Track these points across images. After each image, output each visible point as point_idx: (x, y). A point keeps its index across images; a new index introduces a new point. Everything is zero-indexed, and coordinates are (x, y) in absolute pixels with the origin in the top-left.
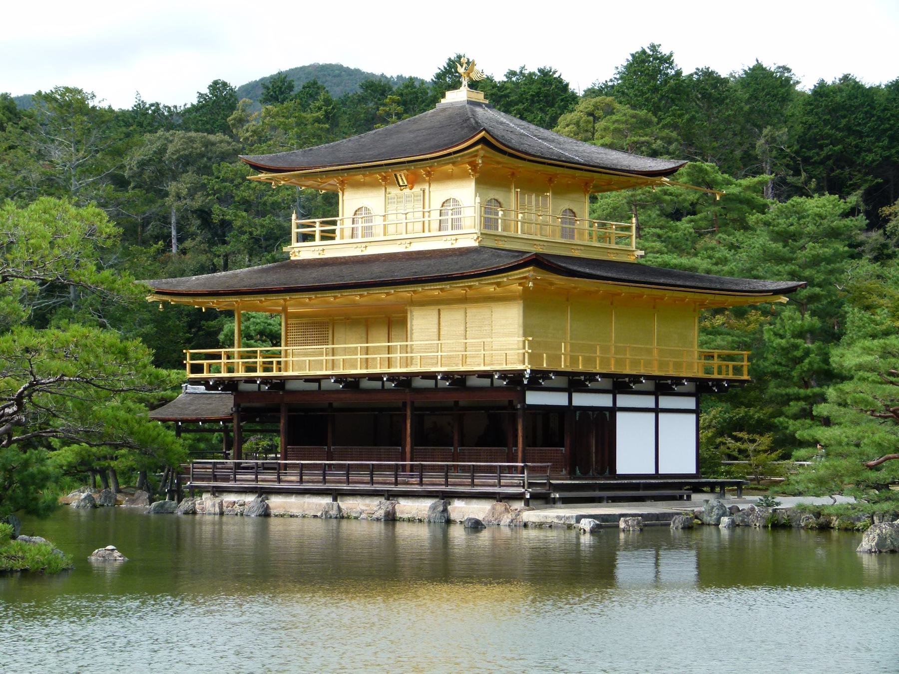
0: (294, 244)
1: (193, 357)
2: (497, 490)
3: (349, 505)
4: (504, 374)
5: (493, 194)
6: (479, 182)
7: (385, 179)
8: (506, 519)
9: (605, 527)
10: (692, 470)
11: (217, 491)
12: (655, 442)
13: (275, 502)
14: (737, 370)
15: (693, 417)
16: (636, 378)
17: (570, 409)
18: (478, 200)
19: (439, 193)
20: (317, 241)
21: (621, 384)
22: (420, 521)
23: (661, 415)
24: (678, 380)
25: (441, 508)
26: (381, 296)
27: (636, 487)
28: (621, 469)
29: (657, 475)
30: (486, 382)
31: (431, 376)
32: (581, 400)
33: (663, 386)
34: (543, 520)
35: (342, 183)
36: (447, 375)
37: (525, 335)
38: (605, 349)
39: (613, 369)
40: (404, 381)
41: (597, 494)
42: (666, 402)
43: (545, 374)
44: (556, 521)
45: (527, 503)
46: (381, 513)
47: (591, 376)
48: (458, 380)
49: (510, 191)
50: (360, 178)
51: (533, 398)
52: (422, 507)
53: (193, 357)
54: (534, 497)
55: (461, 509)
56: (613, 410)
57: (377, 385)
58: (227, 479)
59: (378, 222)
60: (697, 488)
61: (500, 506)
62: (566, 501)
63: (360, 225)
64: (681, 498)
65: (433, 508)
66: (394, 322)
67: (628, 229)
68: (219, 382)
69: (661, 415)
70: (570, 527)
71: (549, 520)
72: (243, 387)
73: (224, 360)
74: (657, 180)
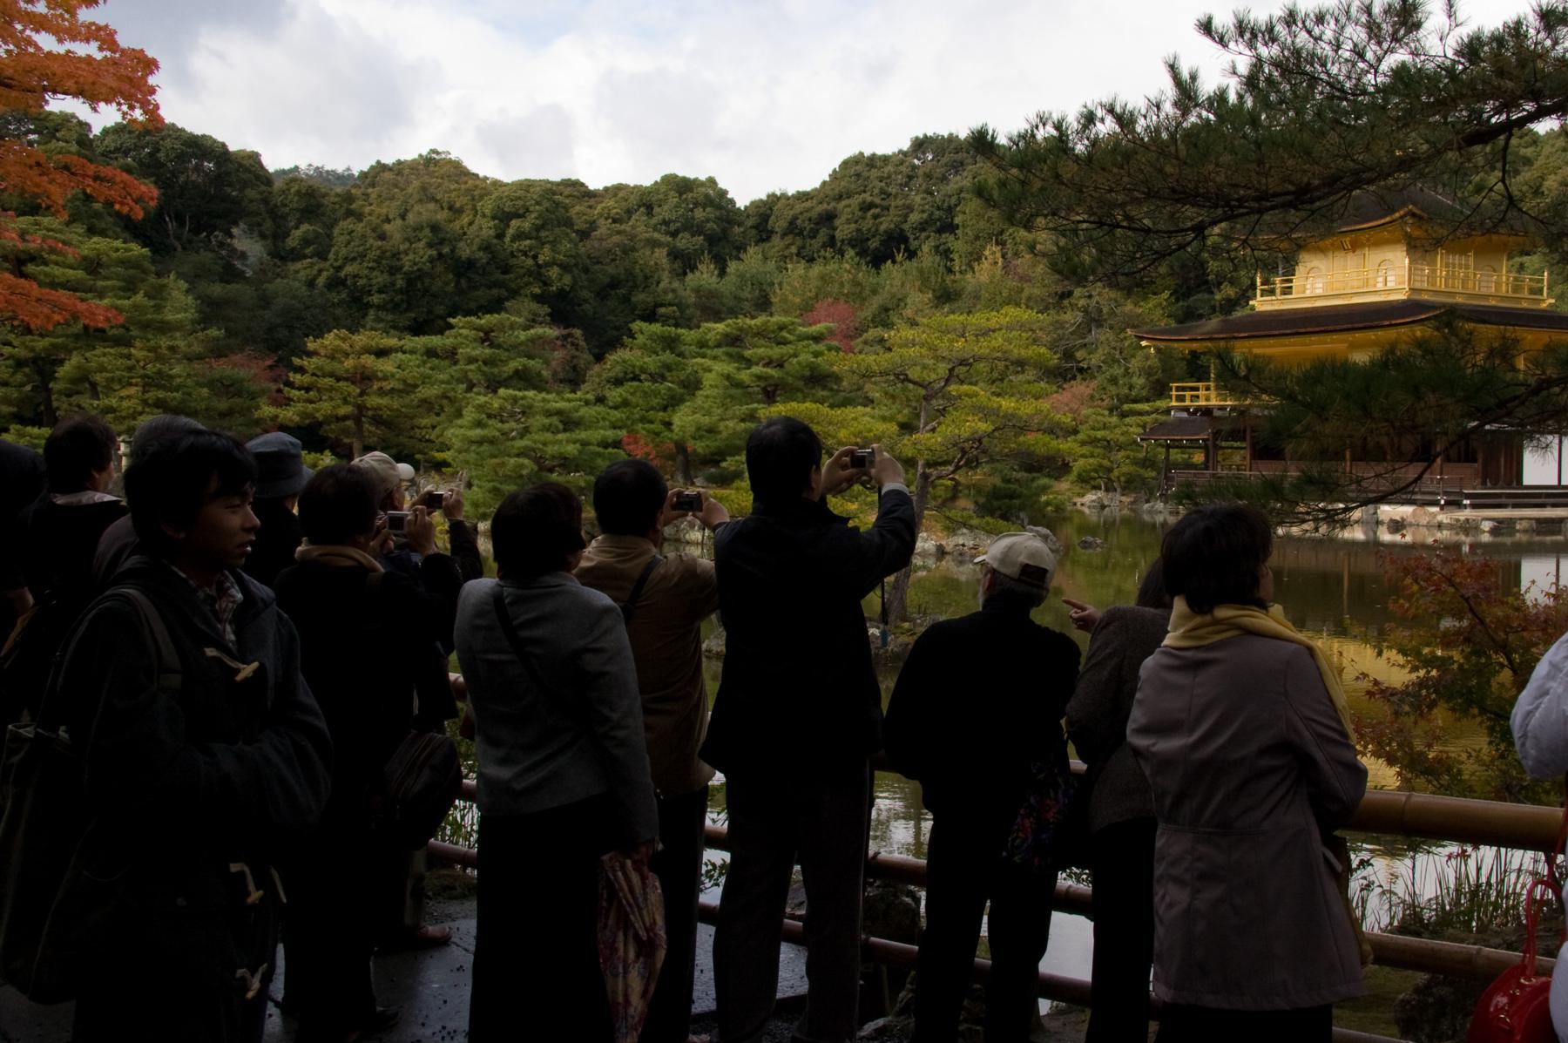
1: (1178, 389)
8: (1424, 521)
9: (1501, 527)
19: (1374, 257)
28: (1527, 481)
29: (1560, 486)
41: (1503, 501)
45: (1442, 508)
53: (1178, 389)
54: (1448, 503)
55: (1388, 511)
61: (1420, 510)
62: (1474, 506)
68: (1198, 409)
72: (1217, 413)
73: (1201, 393)
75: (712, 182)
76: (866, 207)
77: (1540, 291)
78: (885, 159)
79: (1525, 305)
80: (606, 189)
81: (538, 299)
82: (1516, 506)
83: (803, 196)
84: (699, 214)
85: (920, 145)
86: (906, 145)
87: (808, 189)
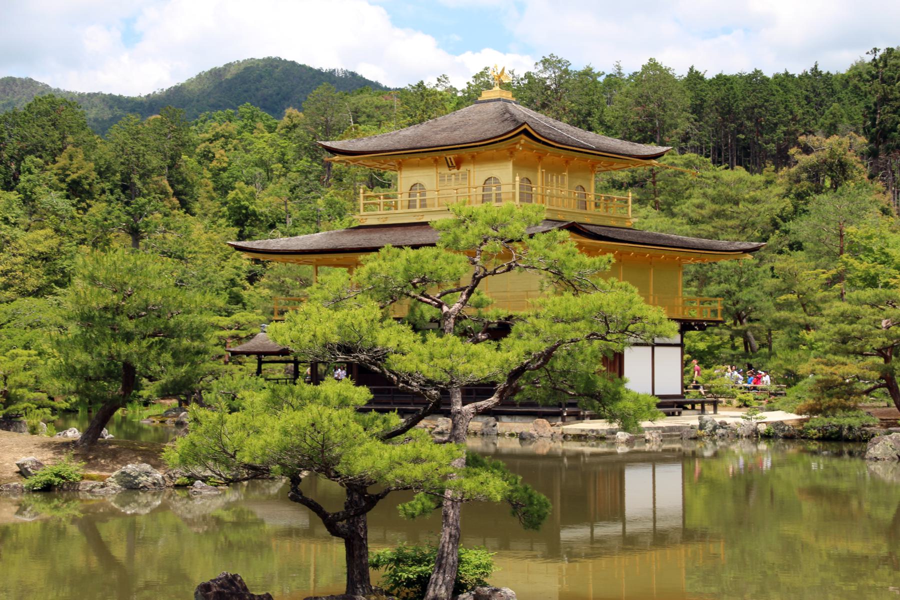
0: (362, 213)
5: (526, 174)
6: (514, 165)
7: (436, 161)
10: (679, 393)
12: (654, 371)
14: (714, 311)
15: (679, 349)
18: (517, 179)
22: (475, 434)
23: (656, 349)
25: (492, 424)
34: (579, 432)
35: (400, 166)
44: (590, 434)
45: (563, 420)
49: (537, 171)
50: (416, 159)
54: (569, 415)
59: (429, 196)
63: (418, 198)
64: (673, 414)
65: (487, 424)
67: (626, 202)
69: (656, 349)
70: (602, 438)
71: (584, 433)
74: (648, 162)
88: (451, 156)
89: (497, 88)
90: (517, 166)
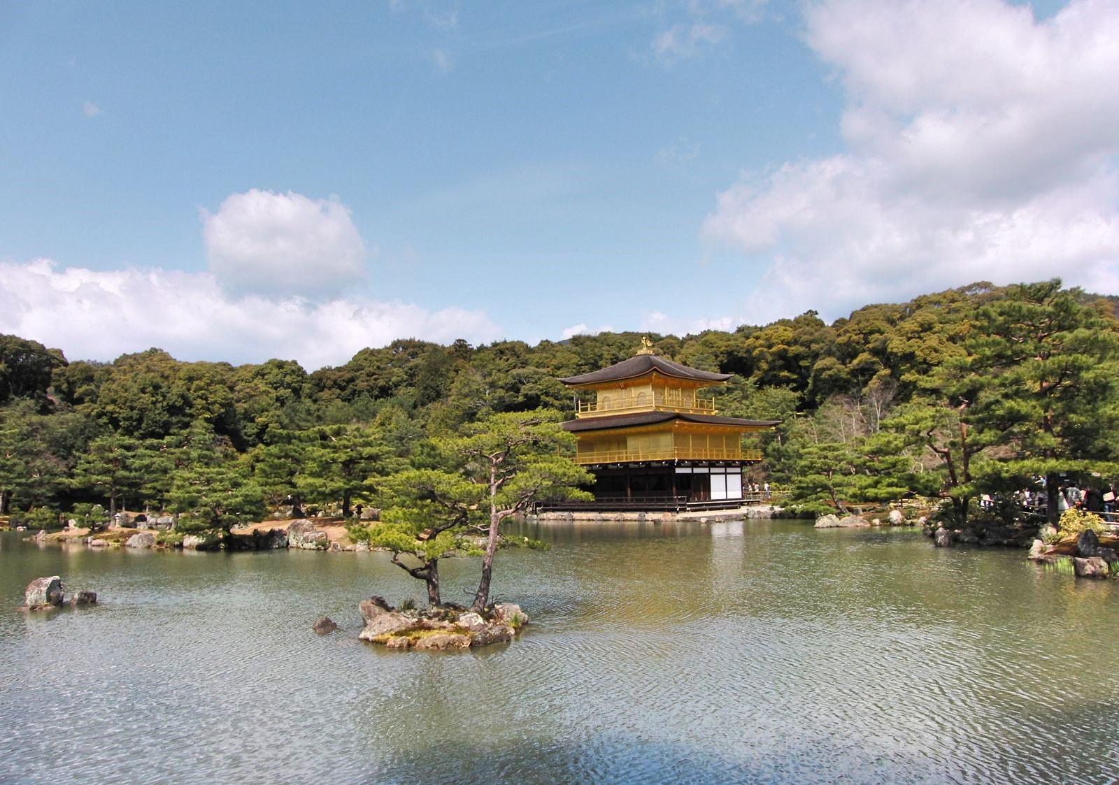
2: (666, 507)
3: (604, 515)
4: (667, 461)
5: (658, 390)
11: (554, 511)
12: (724, 487)
13: (576, 515)
16: (718, 461)
17: (692, 474)
20: (589, 411)
21: (712, 464)
24: (734, 462)
26: (618, 431)
27: (720, 504)
28: (712, 498)
30: (659, 465)
31: (638, 463)
32: (697, 470)
33: (728, 464)
35: (598, 389)
36: (643, 462)
37: (675, 445)
38: (706, 450)
39: (709, 458)
40: (626, 465)
42: (729, 470)
43: (683, 461)
45: (678, 512)
46: (619, 518)
47: (701, 461)
48: (648, 464)
50: (603, 385)
51: (678, 471)
52: (635, 515)
56: (709, 474)
57: (615, 467)
58: (556, 505)
60: (742, 504)
62: (693, 511)
64: (736, 508)
65: (640, 515)
66: (621, 442)
75: (295, 363)
76: (370, 375)
77: (712, 408)
78: (379, 351)
79: (705, 413)
80: (241, 367)
81: (207, 420)
82: (710, 510)
83: (339, 369)
84: (288, 379)
85: (396, 345)
86: (389, 344)
87: (342, 365)
88: (622, 384)
89: (645, 349)
90: (654, 387)
